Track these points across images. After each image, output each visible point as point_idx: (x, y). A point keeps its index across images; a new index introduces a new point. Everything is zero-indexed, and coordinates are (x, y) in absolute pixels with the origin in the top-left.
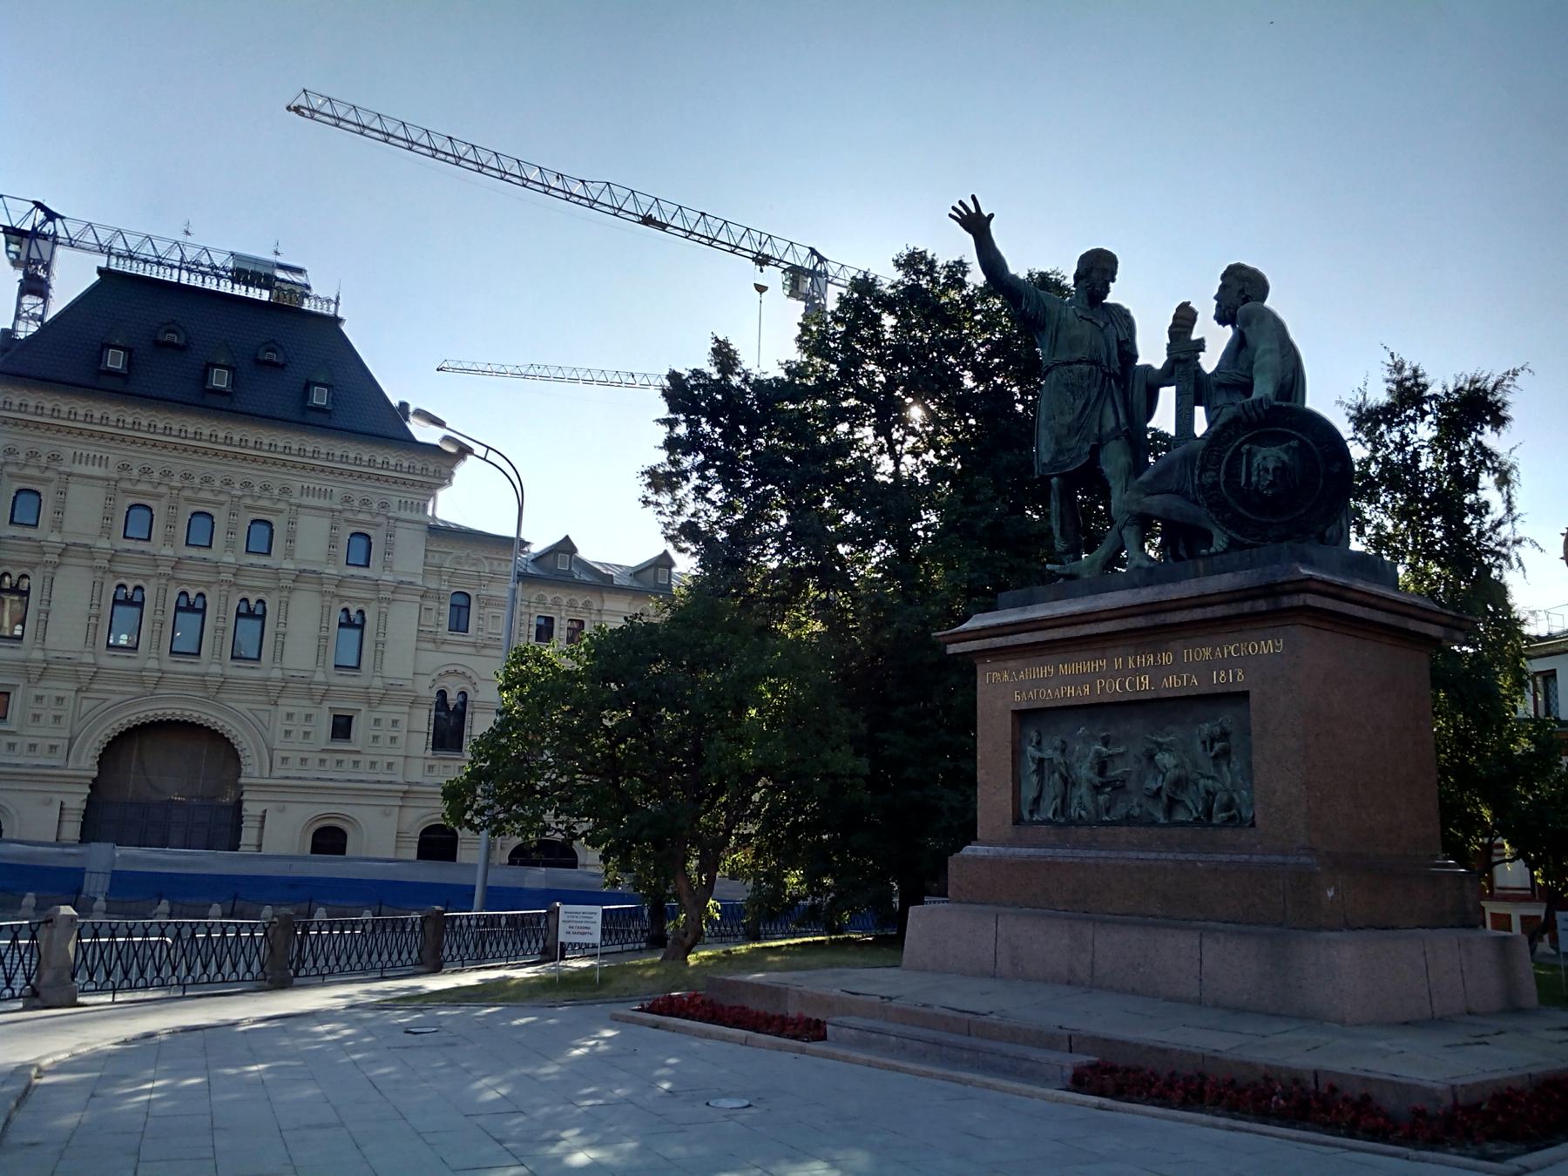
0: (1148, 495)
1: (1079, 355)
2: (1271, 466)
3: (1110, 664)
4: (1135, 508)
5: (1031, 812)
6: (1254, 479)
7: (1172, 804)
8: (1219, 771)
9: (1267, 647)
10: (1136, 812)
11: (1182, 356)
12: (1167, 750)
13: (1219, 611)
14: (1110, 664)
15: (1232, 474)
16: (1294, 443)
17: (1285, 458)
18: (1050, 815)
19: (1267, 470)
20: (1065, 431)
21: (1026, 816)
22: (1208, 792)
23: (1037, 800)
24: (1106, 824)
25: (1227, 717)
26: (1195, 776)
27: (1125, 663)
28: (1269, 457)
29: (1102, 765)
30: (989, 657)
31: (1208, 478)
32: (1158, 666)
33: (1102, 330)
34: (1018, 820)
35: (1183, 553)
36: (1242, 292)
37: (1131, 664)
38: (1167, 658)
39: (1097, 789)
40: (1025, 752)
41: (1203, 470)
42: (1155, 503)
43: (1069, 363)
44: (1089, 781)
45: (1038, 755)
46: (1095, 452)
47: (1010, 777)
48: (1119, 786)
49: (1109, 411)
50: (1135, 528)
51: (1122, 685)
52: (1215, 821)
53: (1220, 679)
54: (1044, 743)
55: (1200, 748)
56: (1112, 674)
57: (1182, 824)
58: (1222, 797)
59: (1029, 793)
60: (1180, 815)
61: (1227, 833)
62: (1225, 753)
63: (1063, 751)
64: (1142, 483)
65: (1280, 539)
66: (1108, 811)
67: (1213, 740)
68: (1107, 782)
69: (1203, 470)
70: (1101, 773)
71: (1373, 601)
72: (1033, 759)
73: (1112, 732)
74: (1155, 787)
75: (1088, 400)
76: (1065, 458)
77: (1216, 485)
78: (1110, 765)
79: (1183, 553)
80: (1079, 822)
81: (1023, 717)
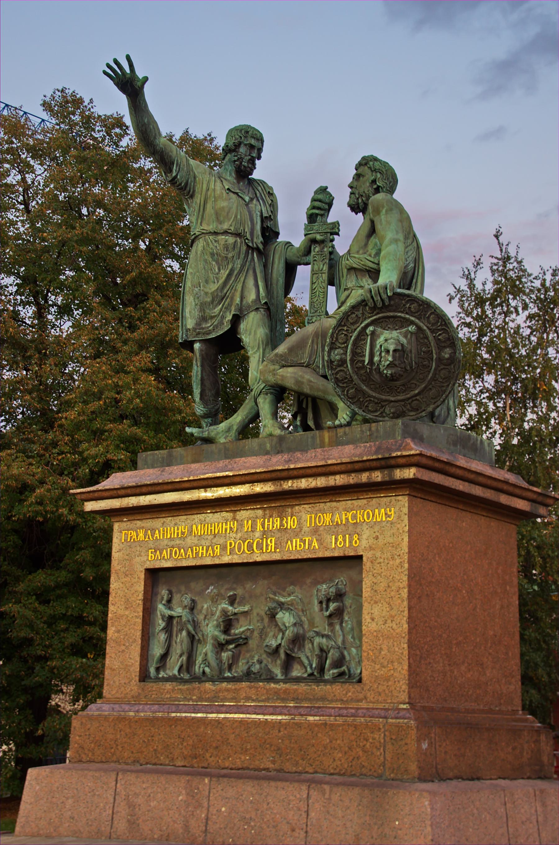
0: (283, 366)
1: (225, 226)
2: (392, 348)
4: (271, 379)
5: (158, 669)
6: (376, 359)
7: (289, 662)
8: (333, 631)
9: (380, 515)
10: (256, 668)
11: (319, 237)
12: (288, 609)
15: (357, 353)
16: (412, 328)
17: (404, 341)
18: (176, 672)
19: (388, 351)
20: (209, 299)
21: (152, 671)
22: (322, 650)
23: (164, 657)
25: (342, 579)
26: (311, 634)
28: (389, 339)
29: (228, 624)
30: (124, 515)
31: (336, 355)
32: (283, 530)
33: (247, 205)
34: (144, 677)
35: (311, 423)
36: (374, 181)
39: (220, 646)
40: (155, 609)
41: (332, 347)
42: (288, 376)
43: (216, 233)
44: (215, 638)
45: (168, 612)
46: (236, 320)
47: (139, 634)
49: (251, 282)
50: (269, 398)
52: (326, 677)
54: (174, 601)
55: (316, 608)
57: (298, 680)
58: (333, 655)
59: (157, 651)
60: (296, 672)
61: (337, 689)
63: (192, 609)
64: (276, 355)
65: (396, 416)
67: (328, 600)
68: (232, 641)
69: (332, 347)
70: (226, 631)
71: (472, 476)
72: (163, 617)
73: (240, 591)
74: (274, 643)
75: (232, 271)
76: (208, 325)
77: (343, 362)
78: (235, 623)
79: (311, 423)
80: (202, 678)
81: (154, 575)
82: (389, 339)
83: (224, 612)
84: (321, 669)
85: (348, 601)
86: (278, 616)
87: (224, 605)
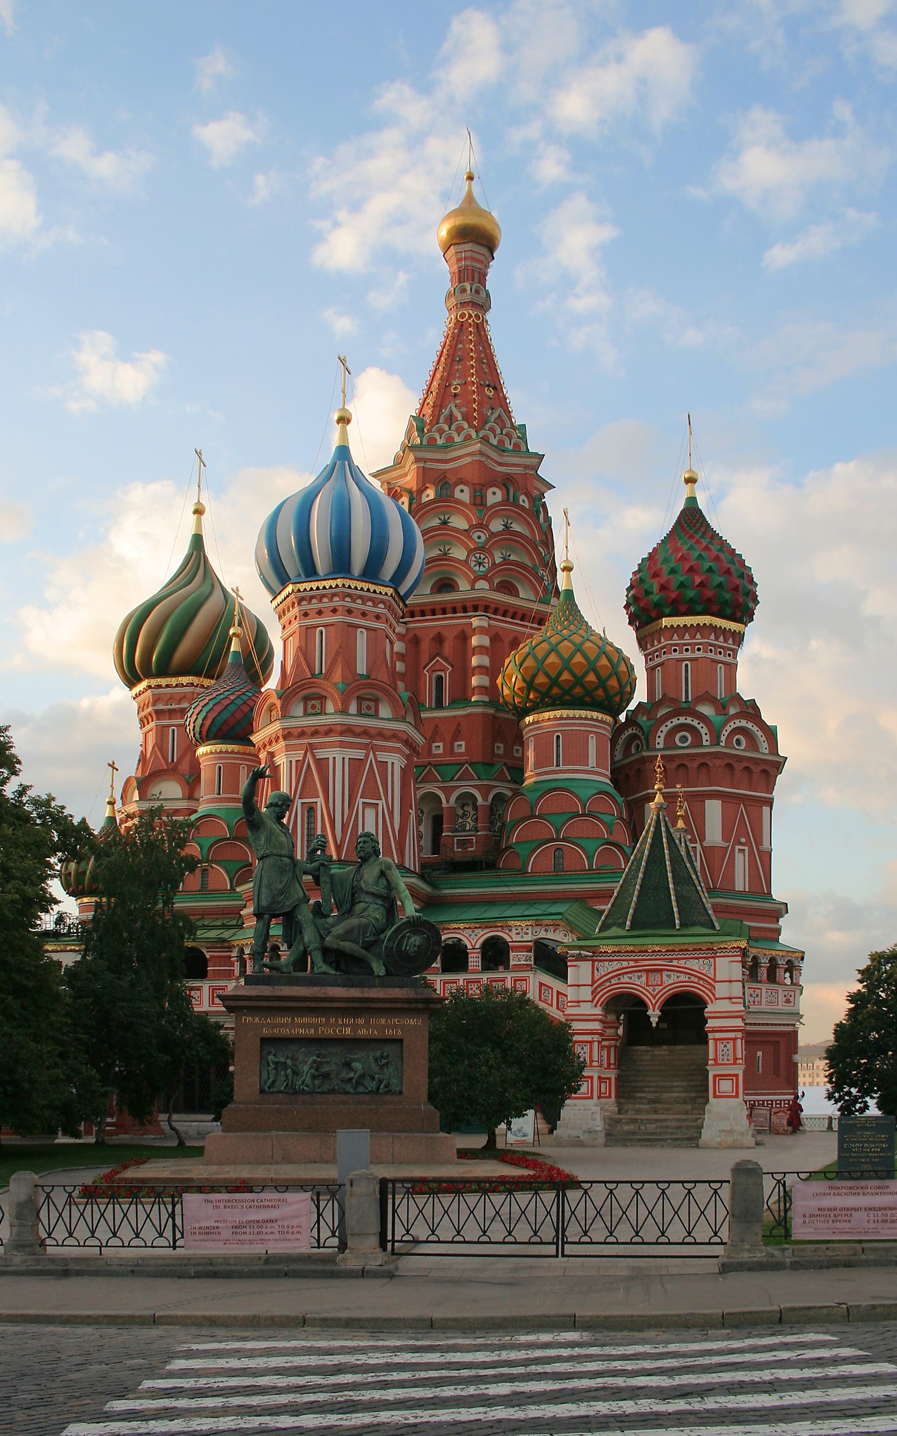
3: (328, 1020)
9: (412, 1022)
10: (337, 1088)
13: (399, 1005)
14: (328, 1020)
24: (319, 1093)
25: (389, 1049)
27: (337, 1021)
37: (340, 1022)
38: (361, 1021)
39: (314, 1077)
48: (326, 1076)
50: (320, 953)
51: (334, 1031)
53: (389, 1033)
55: (372, 1060)
56: (327, 1024)
57: (362, 1093)
60: (361, 1089)
61: (388, 1098)
62: (387, 1064)
66: (319, 1087)
69: (389, 940)
73: (323, 1052)
77: (392, 947)
82: (416, 940)
83: (315, 1062)
84: (378, 1089)
85: (391, 1059)
86: (353, 1064)
87: (315, 1058)
